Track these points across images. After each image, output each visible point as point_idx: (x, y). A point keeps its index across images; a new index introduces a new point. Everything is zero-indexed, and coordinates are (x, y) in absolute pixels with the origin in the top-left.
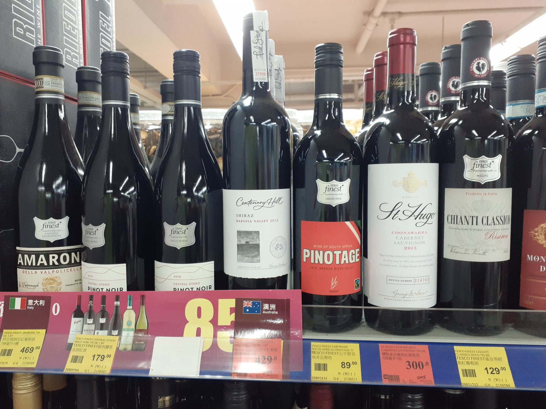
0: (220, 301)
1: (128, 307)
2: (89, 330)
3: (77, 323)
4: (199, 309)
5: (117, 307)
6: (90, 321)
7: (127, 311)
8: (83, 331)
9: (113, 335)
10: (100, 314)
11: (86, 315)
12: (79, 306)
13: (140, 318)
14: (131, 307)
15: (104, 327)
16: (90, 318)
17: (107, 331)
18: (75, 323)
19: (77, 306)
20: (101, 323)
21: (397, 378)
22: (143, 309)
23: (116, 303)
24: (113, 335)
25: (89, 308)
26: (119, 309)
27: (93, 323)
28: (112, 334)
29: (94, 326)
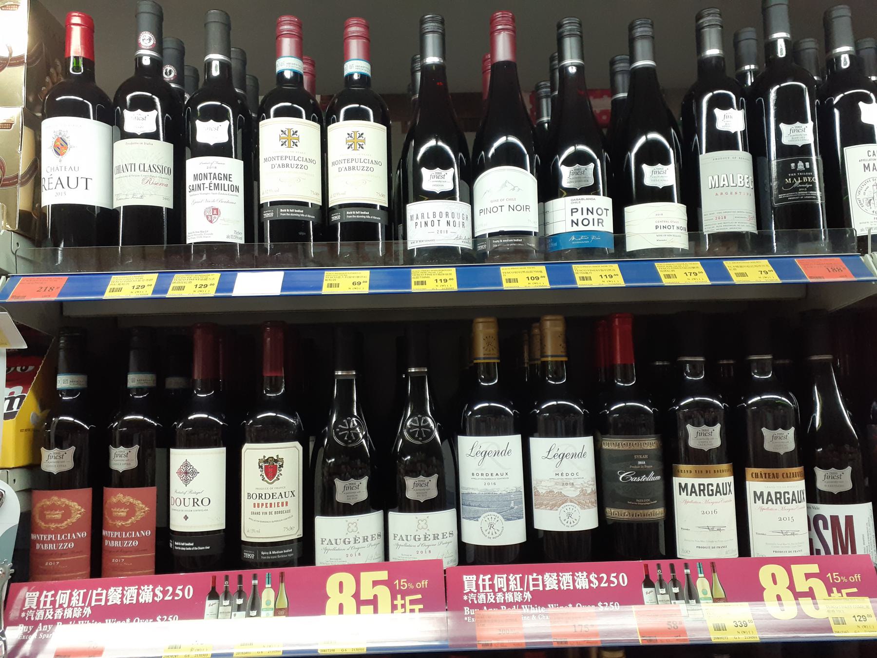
2: (226, 612)
3: (212, 605)
8: (219, 614)
9: (252, 616)
11: (222, 596)
12: (214, 588)
13: (279, 600)
17: (245, 612)
18: (209, 606)
19: (212, 587)
20: (238, 605)
23: (253, 582)
24: (252, 616)
25: (224, 590)
28: (251, 615)
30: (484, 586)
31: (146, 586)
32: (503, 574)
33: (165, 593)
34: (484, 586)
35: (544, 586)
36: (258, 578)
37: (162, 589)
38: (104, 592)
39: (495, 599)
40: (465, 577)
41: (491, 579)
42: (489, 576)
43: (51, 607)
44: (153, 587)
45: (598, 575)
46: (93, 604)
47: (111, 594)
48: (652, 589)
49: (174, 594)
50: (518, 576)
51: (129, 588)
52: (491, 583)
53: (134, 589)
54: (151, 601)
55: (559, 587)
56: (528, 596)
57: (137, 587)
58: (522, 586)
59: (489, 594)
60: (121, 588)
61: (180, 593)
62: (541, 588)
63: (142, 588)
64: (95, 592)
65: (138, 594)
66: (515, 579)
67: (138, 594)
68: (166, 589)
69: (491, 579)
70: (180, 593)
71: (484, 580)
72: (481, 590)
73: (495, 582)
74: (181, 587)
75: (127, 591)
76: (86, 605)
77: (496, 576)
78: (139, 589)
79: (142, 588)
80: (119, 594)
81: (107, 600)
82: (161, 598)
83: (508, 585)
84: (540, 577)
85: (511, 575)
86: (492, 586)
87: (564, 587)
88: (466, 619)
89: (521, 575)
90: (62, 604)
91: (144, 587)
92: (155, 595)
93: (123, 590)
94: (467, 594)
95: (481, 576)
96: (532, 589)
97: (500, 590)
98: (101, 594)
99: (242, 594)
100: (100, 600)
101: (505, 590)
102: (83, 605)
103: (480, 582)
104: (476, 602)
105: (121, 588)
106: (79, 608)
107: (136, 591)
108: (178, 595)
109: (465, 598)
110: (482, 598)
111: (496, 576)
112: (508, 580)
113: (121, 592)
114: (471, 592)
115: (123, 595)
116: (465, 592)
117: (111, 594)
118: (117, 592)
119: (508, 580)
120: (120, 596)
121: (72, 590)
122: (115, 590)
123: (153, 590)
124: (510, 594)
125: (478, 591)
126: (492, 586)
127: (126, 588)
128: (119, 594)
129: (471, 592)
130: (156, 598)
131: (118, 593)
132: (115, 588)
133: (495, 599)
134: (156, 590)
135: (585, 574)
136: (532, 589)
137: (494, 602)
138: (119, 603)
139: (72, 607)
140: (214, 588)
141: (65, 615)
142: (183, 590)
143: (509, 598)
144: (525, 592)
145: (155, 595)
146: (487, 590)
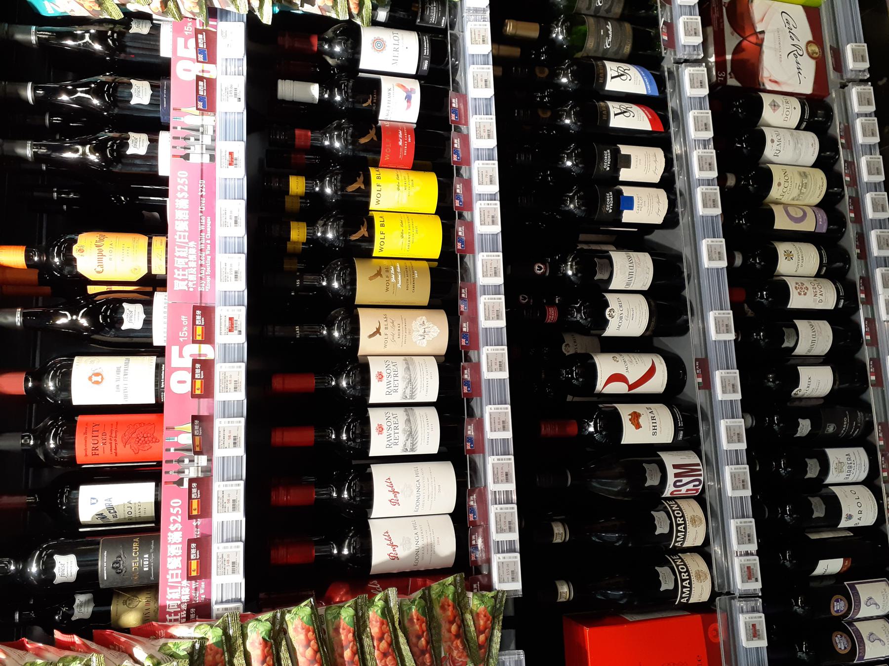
0: (173, 366)
1: (176, 440)
4: (180, 382)
5: (175, 450)
6: (187, 471)
7: (179, 441)
10: (181, 464)
12: (174, 483)
14: (176, 438)
15: (191, 459)
16: (184, 472)
22: (177, 428)
25: (176, 474)
26: (177, 448)
27: (189, 468)
29: (190, 468)
30: (183, 275)
32: (174, 260)
33: (175, 522)
34: (183, 275)
35: (185, 231)
36: (169, 448)
37: (172, 525)
39: (193, 268)
40: (175, 289)
41: (178, 269)
42: (176, 271)
43: (179, 614)
45: (178, 191)
46: (179, 579)
48: (191, 155)
49: (177, 514)
50: (177, 249)
52: (181, 270)
54: (181, 533)
55: (186, 220)
56: (192, 244)
58: (184, 247)
59: (189, 272)
61: (176, 509)
62: (187, 234)
64: (170, 580)
65: (175, 543)
66: (179, 251)
67: (175, 543)
68: (172, 521)
69: (178, 269)
70: (176, 509)
71: (179, 275)
72: (186, 277)
73: (181, 267)
74: (171, 510)
76: (180, 585)
77: (176, 265)
78: (170, 544)
81: (178, 568)
82: (180, 525)
83: (183, 257)
84: (178, 233)
85: (175, 254)
86: (184, 269)
87: (187, 217)
88: (207, 290)
89: (176, 247)
90: (177, 605)
92: (176, 530)
93: (170, 557)
94: (189, 288)
95: (176, 276)
96: (186, 240)
97: (187, 264)
98: (172, 575)
99: (180, 459)
100: (177, 574)
101: (187, 260)
102: (180, 588)
103: (180, 277)
104: (195, 282)
106: (182, 590)
107: (172, 546)
108: (178, 511)
109: (191, 290)
110: (193, 278)
111: (176, 265)
112: (179, 257)
114: (187, 285)
115: (175, 556)
116: (187, 290)
119: (179, 257)
120: (175, 558)
121: (167, 599)
123: (172, 532)
124: (190, 256)
125: (187, 279)
126: (184, 269)
127: (168, 555)
129: (187, 285)
130: (179, 529)
133: (193, 268)
134: (172, 529)
135: (177, 200)
136: (186, 240)
137: (195, 269)
138: (181, 558)
139: (180, 597)
140: (174, 483)
141: (186, 601)
142: (174, 508)
143: (193, 257)
144: (189, 246)
145: (176, 530)
146: (186, 273)
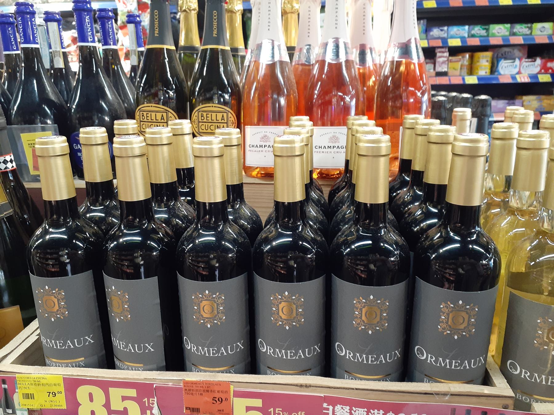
21: (486, 399)
31: (376, 411)
38: (331, 408)
44: (383, 412)
47: (338, 410)
51: (357, 409)
53: (362, 411)
57: (366, 410)
60: (348, 408)
63: (371, 411)
75: (355, 411)
79: (371, 411)
80: (347, 412)
91: (374, 410)
93: (351, 409)
105: (348, 408)
113: (349, 411)
117: (338, 410)
118: (344, 410)
122: (342, 408)
127: (354, 408)
128: (347, 412)
131: (345, 411)
132: (342, 406)
